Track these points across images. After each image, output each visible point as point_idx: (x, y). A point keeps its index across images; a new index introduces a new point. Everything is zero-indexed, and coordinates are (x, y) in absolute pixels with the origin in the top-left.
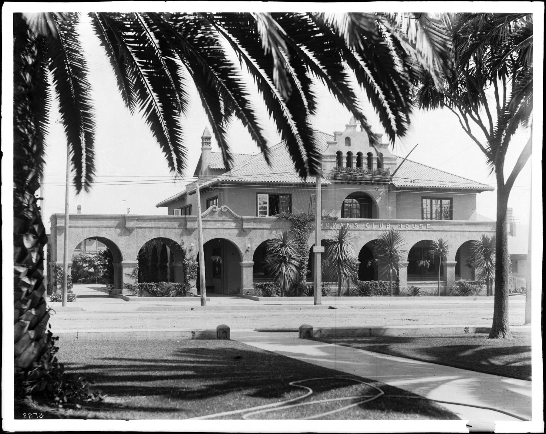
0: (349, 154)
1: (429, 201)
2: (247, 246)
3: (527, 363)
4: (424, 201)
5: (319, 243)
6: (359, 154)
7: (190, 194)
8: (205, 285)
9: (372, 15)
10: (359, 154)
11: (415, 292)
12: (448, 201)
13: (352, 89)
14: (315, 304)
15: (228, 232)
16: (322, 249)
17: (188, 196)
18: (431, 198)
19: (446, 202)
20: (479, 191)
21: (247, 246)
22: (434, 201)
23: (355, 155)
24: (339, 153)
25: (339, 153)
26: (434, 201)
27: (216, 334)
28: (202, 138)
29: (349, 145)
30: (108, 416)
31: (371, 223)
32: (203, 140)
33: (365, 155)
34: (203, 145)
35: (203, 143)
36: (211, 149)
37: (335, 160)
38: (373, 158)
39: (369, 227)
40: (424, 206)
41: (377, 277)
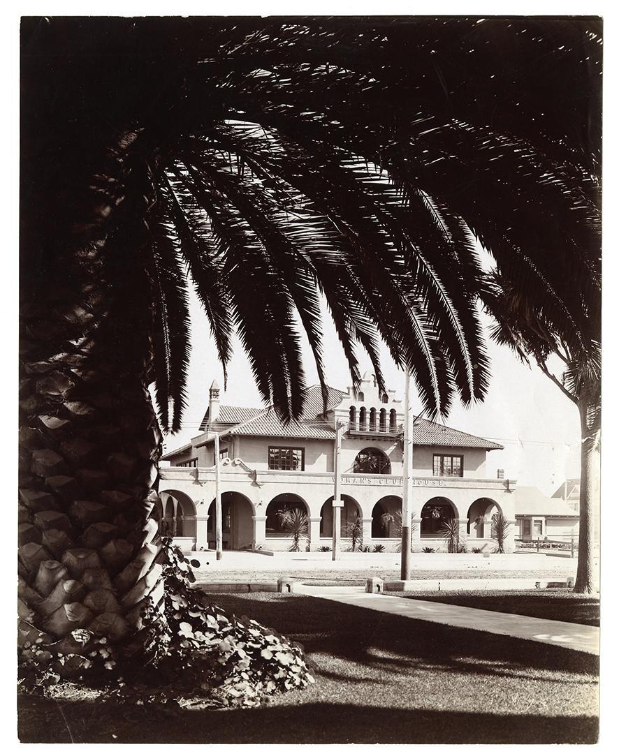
0: (363, 409)
1: (449, 459)
2: (261, 498)
3: (598, 604)
4: (435, 457)
5: (339, 497)
6: (373, 410)
7: (197, 447)
8: (221, 539)
9: (512, 342)
10: (373, 410)
11: (379, 549)
12: (459, 459)
13: (485, 391)
14: (334, 559)
15: (243, 487)
16: (342, 503)
17: (194, 449)
18: (452, 456)
19: (457, 461)
20: (489, 449)
21: (261, 498)
22: (454, 458)
23: (368, 410)
24: (352, 408)
25: (352, 408)
26: (454, 458)
27: (277, 587)
28: (211, 390)
29: (363, 401)
30: (537, 593)
31: (387, 478)
32: (211, 393)
33: (378, 411)
34: (211, 398)
35: (211, 396)
36: (219, 401)
37: (348, 414)
38: (386, 414)
39: (383, 482)
40: (445, 463)
41: (388, 533)
